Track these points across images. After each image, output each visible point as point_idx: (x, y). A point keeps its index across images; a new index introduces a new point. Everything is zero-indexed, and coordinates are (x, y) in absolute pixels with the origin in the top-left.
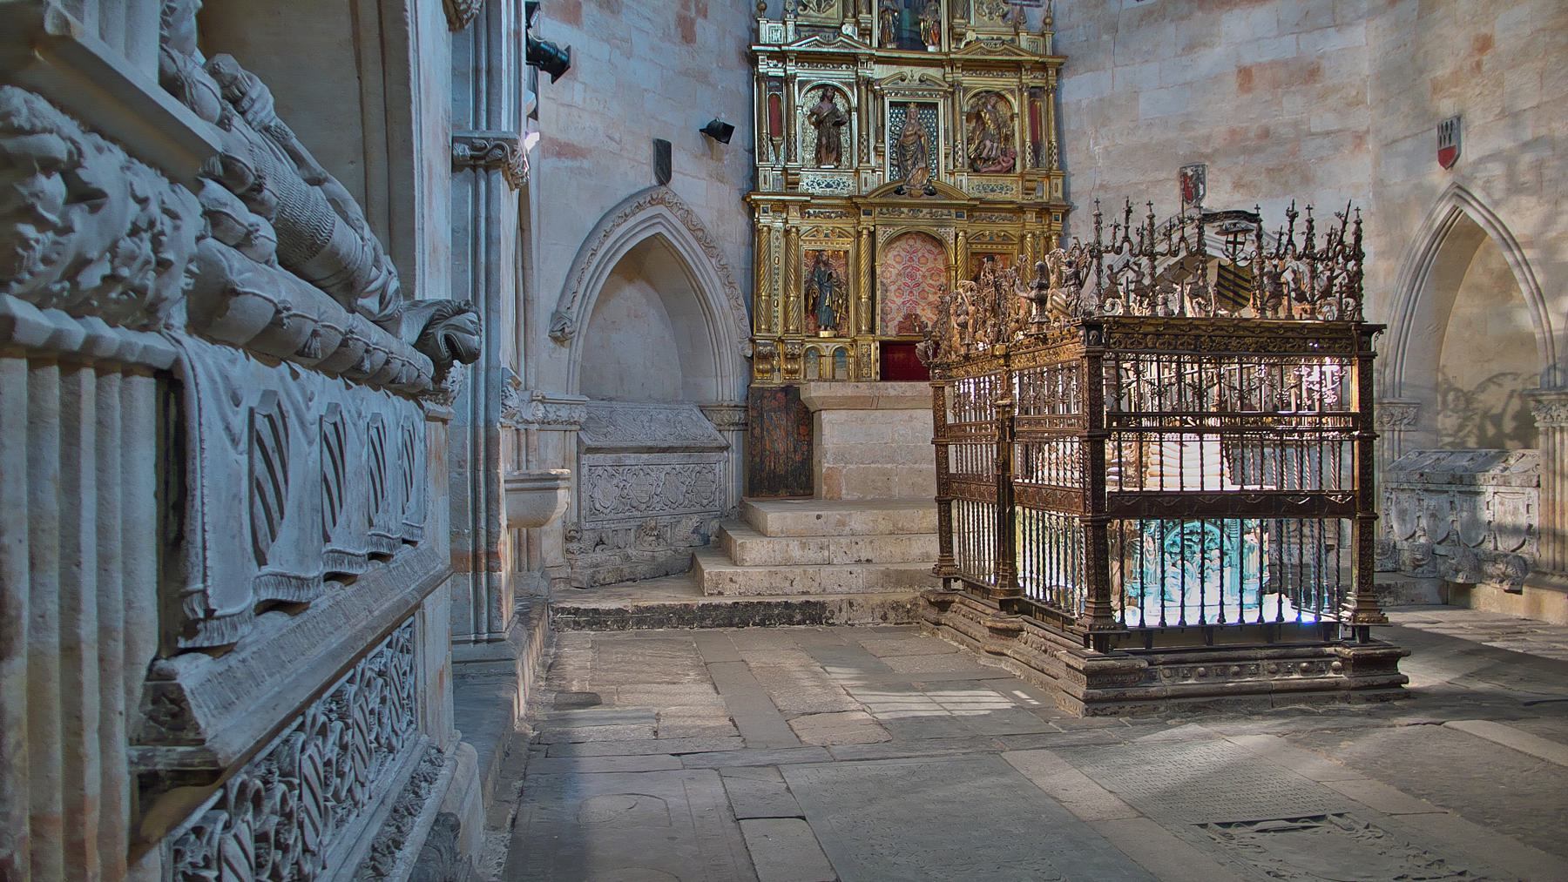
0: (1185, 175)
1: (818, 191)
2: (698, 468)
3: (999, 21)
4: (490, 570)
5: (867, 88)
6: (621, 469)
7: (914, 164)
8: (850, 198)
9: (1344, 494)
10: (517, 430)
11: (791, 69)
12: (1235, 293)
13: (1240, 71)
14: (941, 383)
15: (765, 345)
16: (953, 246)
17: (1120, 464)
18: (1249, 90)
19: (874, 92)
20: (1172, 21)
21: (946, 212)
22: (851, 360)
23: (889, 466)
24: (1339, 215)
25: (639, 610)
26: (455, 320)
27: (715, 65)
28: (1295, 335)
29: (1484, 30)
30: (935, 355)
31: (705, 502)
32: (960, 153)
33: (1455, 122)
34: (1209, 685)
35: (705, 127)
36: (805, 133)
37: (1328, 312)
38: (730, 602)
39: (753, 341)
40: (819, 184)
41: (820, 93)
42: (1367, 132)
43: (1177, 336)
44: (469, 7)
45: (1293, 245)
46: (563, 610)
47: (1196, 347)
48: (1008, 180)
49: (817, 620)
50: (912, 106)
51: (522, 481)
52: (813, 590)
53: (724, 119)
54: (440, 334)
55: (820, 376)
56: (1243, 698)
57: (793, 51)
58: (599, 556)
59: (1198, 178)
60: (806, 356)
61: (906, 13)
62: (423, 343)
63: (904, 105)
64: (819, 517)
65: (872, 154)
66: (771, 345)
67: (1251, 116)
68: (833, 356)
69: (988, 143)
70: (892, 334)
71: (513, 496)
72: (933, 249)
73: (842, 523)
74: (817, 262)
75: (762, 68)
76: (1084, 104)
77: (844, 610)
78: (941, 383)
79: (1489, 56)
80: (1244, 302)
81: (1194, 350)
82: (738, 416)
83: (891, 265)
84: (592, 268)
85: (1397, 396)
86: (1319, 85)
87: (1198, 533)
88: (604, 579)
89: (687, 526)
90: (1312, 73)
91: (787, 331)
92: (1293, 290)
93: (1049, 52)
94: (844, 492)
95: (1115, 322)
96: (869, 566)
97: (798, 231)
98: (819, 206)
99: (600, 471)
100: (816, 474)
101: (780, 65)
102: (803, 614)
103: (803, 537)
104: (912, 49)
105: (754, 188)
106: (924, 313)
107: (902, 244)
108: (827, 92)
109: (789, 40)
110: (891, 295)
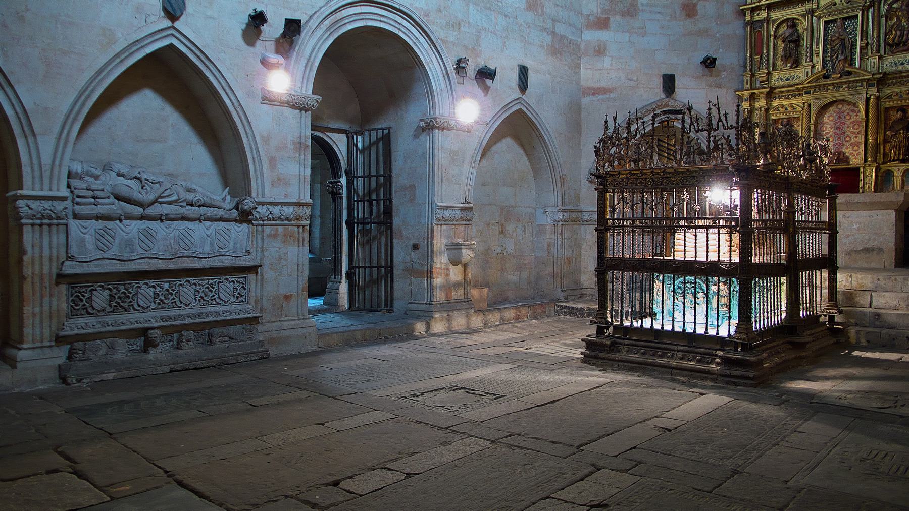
4: (431, 278)
35: (702, 60)
40: (781, 79)
46: (560, 306)
51: (452, 246)
56: (656, 368)
71: (449, 251)
87: (691, 283)
92: (697, 149)
106: (847, 151)
108: (792, 23)
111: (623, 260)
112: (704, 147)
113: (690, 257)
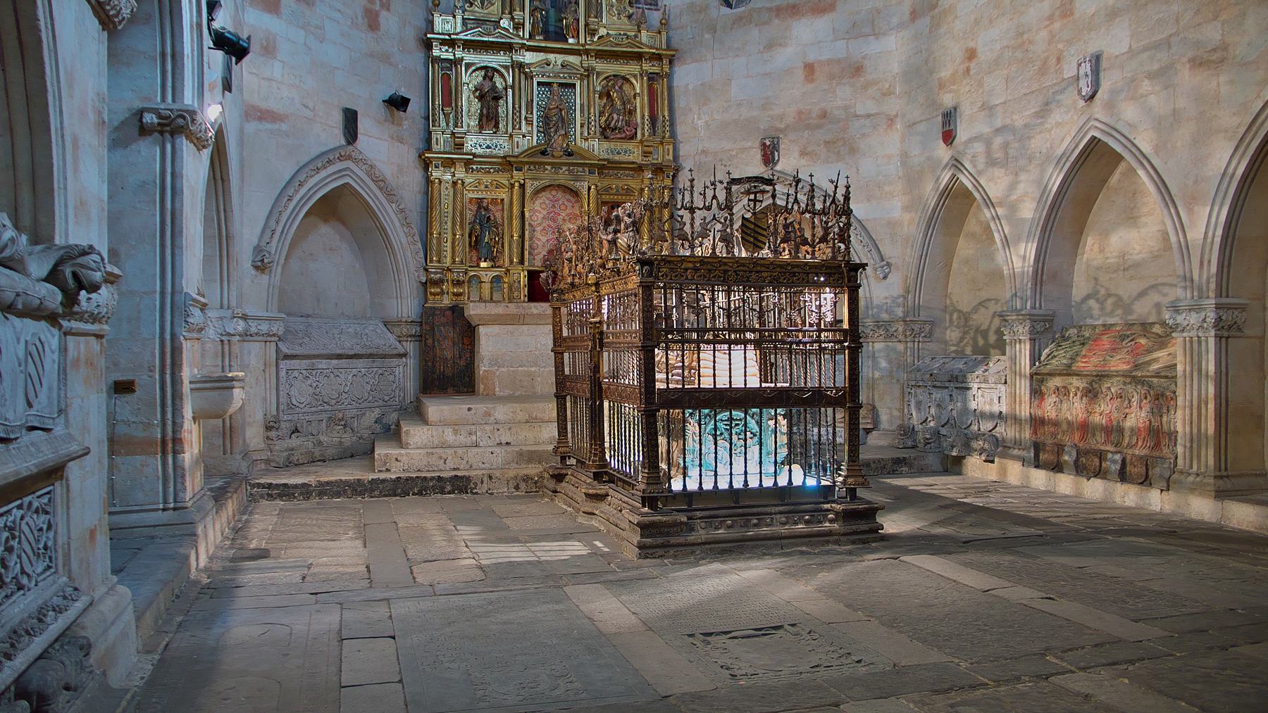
0: (764, 144)
1: (479, 151)
2: (380, 371)
3: (626, 20)
4: (175, 453)
5: (519, 70)
6: (314, 372)
7: (556, 132)
8: (505, 157)
9: (838, 390)
10: (222, 341)
11: (459, 54)
12: (756, 239)
13: (805, 67)
14: (558, 304)
15: (435, 273)
16: (586, 196)
17: (683, 367)
18: (812, 81)
19: (525, 74)
20: (756, 25)
21: (581, 169)
22: (506, 285)
23: (533, 369)
24: (832, 182)
25: (321, 484)
26: (80, 260)
27: (396, 49)
28: (800, 270)
29: (971, 44)
30: (553, 283)
31: (387, 398)
32: (593, 123)
33: (952, 111)
34: (735, 534)
35: (387, 98)
36: (469, 104)
37: (823, 253)
38: (394, 477)
39: (426, 270)
40: (480, 146)
41: (483, 73)
42: (897, 115)
43: (710, 270)
44: (119, 12)
45: (798, 203)
46: (259, 485)
47: (724, 279)
48: (630, 146)
49: (464, 490)
50: (555, 85)
51: (204, 382)
52: (462, 467)
53: (404, 92)
54: (68, 271)
55: (481, 298)
56: (760, 543)
57: (460, 40)
58: (294, 442)
59: (774, 147)
60: (469, 282)
61: (552, 12)
62: (53, 277)
63: (549, 84)
64: (469, 409)
65: (524, 122)
66: (442, 273)
67: (813, 101)
68: (491, 282)
69: (615, 116)
70: (538, 264)
71: (196, 394)
72: (571, 198)
73: (488, 414)
74: (479, 208)
75: (436, 52)
76: (690, 87)
77: (485, 482)
78: (558, 304)
79: (974, 64)
80: (762, 245)
81: (724, 281)
82: (415, 330)
83: (538, 210)
84: (288, 211)
85: (917, 315)
86: (862, 79)
88: (298, 460)
89: (370, 417)
90: (858, 70)
91: (454, 262)
93: (664, 47)
94: (497, 389)
95: (663, 260)
96: (509, 449)
97: (463, 183)
98: (480, 163)
99: (296, 374)
100: (476, 376)
101: (450, 50)
102: (453, 486)
103: (455, 425)
104: (556, 40)
105: (429, 148)
107: (546, 194)
108: (489, 72)
109: (459, 30)
110: (538, 234)
111: (715, 391)
112: (808, 235)
113: (722, 383)
